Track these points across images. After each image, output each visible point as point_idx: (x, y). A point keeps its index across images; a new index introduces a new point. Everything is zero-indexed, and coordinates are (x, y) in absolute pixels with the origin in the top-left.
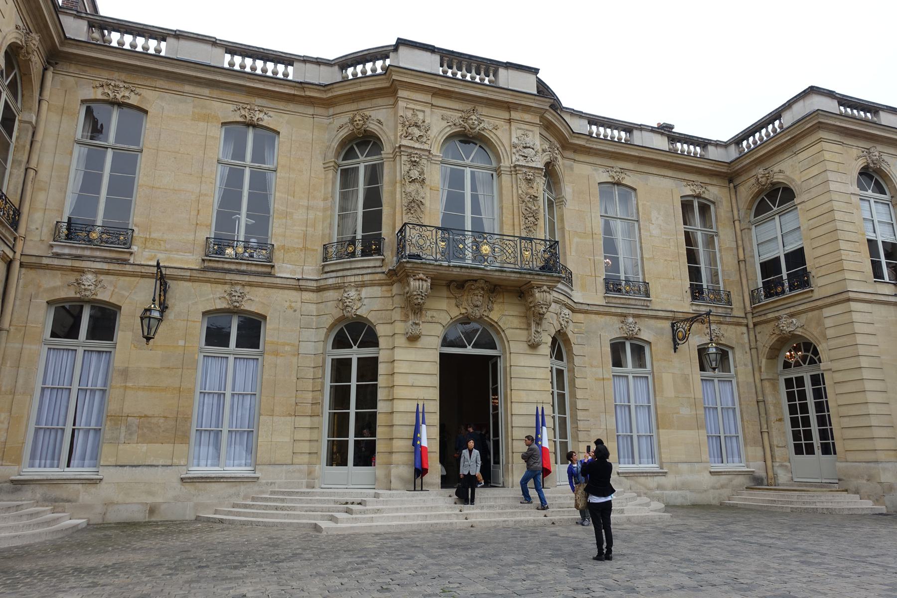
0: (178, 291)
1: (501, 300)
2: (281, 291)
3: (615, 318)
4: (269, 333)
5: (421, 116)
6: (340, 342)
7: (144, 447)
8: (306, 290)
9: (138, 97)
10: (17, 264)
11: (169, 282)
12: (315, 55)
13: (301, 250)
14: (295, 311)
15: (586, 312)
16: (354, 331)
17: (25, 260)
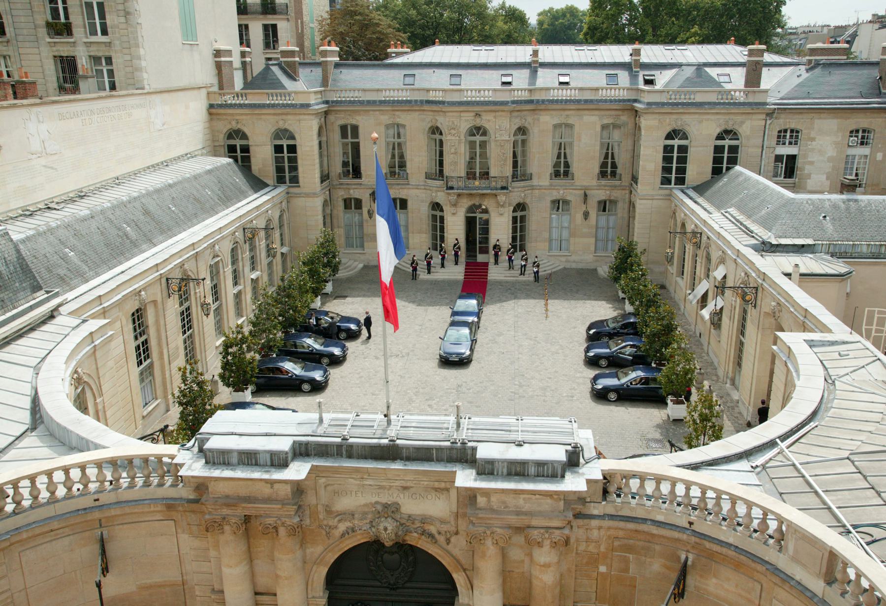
4: (410, 204)
16: (436, 206)
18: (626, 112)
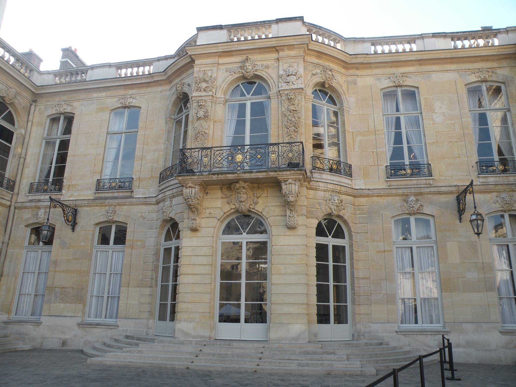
0: (83, 212)
1: (265, 195)
2: (137, 207)
3: (398, 198)
5: (209, 74)
6: (168, 238)
7: (62, 305)
8: (150, 204)
9: (71, 107)
10: (12, 208)
11: (79, 209)
12: (163, 54)
13: (150, 179)
14: (144, 219)
15: (367, 196)
17: (17, 205)
18: (504, 63)
